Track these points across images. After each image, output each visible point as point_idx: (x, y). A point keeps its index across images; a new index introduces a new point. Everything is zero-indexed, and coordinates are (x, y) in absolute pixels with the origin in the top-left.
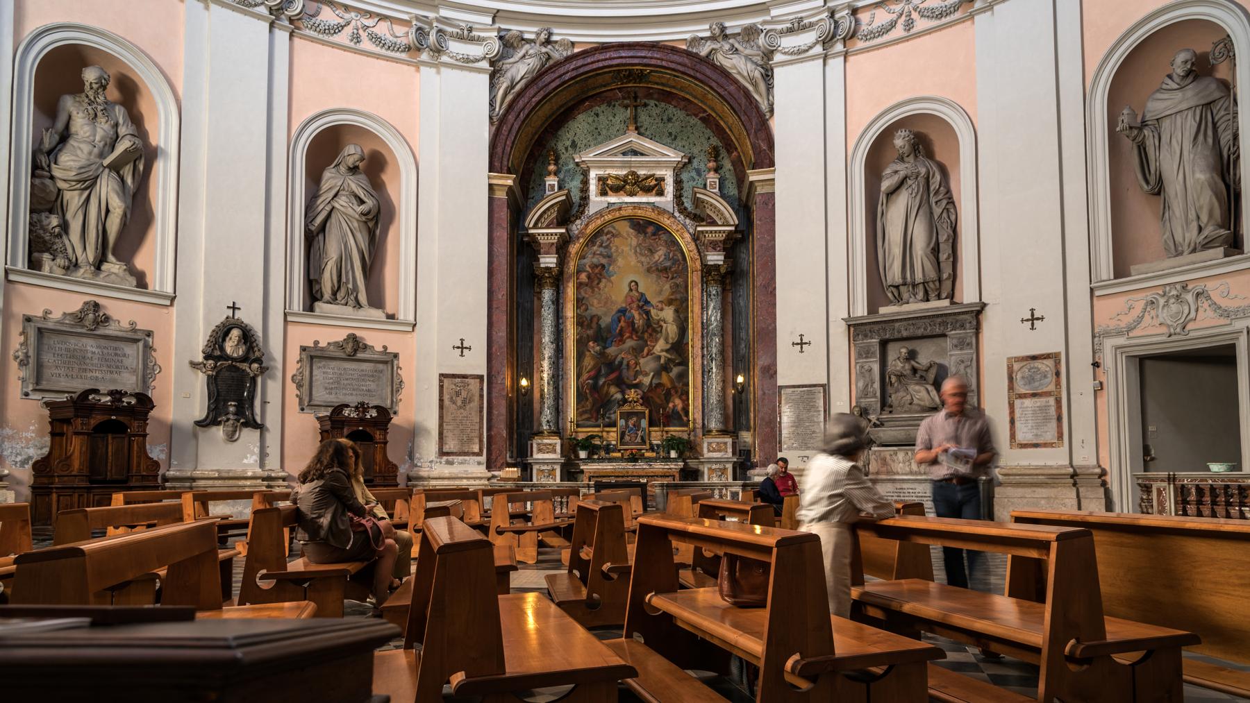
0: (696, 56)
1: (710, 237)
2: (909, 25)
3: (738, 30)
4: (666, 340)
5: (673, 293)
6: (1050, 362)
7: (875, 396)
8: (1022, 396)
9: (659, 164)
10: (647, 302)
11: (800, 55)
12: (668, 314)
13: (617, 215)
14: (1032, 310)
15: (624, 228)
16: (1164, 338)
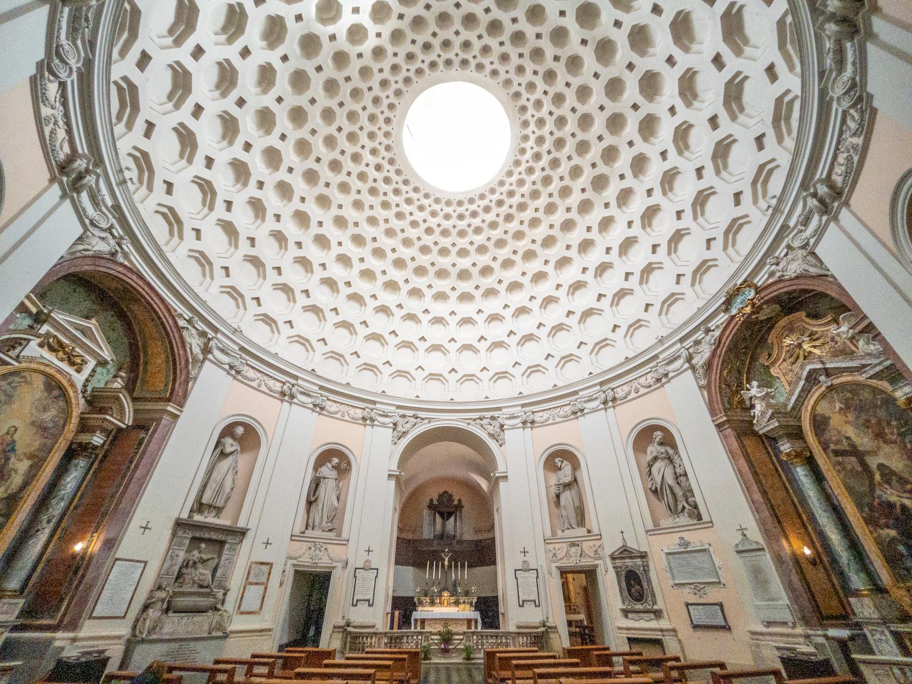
0: (176, 323)
1: (105, 425)
2: (260, 385)
3: (200, 329)
4: (6, 489)
5: (38, 450)
6: (268, 567)
8: (251, 584)
9: (92, 352)
10: (13, 450)
11: (218, 364)
12: (23, 466)
13: (42, 368)
15: (39, 381)
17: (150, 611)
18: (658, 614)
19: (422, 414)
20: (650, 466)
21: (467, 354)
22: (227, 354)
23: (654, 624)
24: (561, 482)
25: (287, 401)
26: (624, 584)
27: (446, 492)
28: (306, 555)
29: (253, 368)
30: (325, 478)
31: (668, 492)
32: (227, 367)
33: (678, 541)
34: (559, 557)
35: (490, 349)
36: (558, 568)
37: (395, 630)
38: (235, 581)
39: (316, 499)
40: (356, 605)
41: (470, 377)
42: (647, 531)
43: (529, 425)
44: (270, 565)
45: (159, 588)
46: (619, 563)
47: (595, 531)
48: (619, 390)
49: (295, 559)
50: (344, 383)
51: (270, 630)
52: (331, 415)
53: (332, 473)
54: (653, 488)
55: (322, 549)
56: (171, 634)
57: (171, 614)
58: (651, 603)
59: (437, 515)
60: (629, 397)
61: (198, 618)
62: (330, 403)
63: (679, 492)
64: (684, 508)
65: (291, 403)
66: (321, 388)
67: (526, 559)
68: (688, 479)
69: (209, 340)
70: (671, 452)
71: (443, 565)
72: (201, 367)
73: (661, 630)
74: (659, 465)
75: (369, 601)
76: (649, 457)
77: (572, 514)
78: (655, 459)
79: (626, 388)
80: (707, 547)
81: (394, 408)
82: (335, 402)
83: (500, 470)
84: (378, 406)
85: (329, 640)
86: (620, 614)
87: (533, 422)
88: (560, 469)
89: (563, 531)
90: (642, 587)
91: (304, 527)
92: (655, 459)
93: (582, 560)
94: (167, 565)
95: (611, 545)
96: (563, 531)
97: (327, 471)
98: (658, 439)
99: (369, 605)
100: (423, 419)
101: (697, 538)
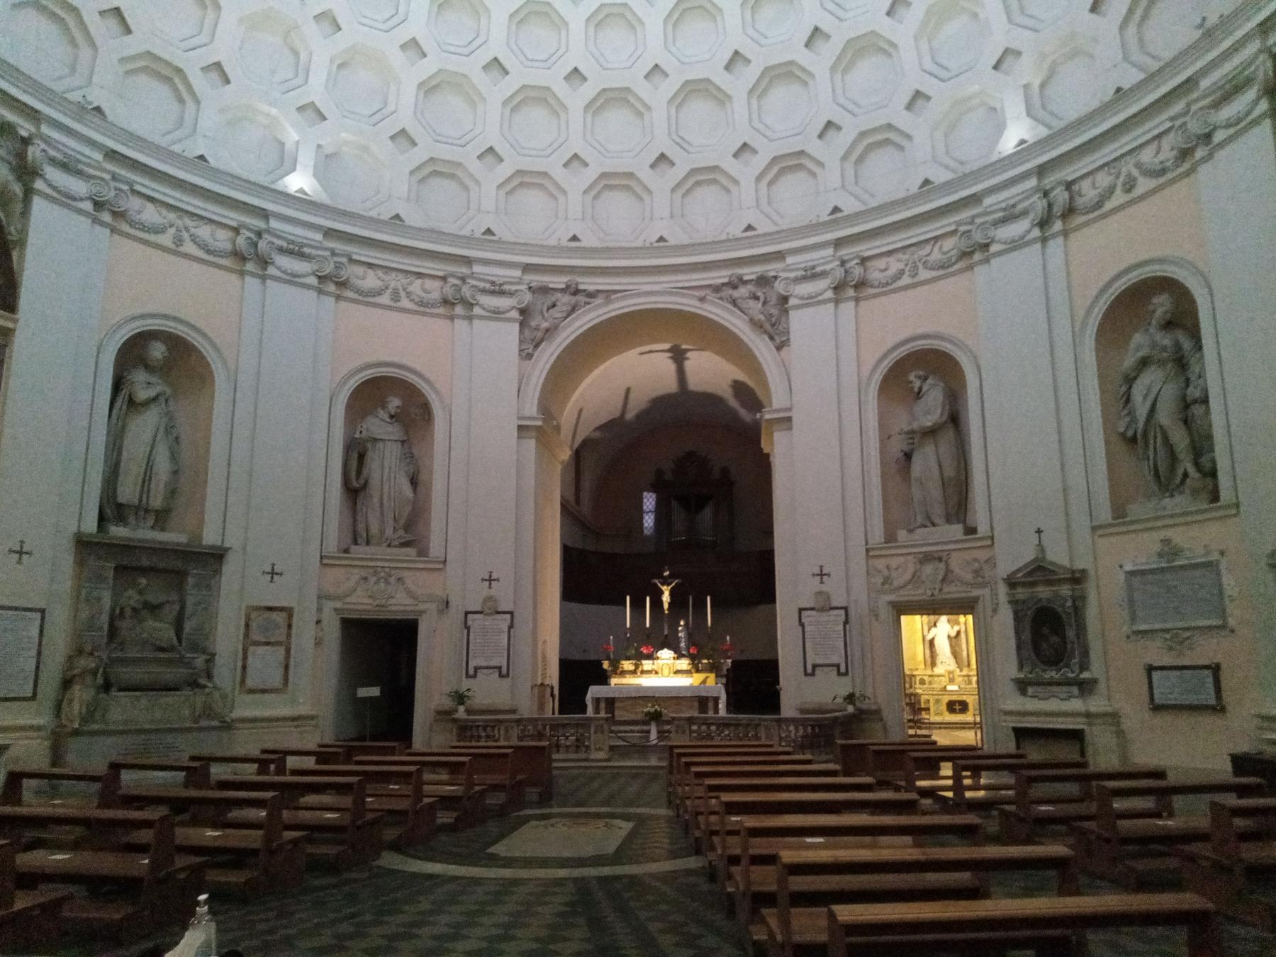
2: (179, 241)
6: (284, 614)
7: (101, 629)
11: (65, 199)
14: (273, 565)
16: (368, 607)
17: (76, 688)
18: (1086, 688)
19: (588, 283)
20: (1130, 380)
21: (699, 108)
22: (79, 173)
23: (1076, 705)
24: (915, 426)
25: (253, 274)
26: (1027, 636)
27: (691, 454)
28: (359, 592)
29: (151, 199)
30: (376, 440)
31: (1159, 440)
32: (88, 206)
33: (1157, 547)
34: (896, 584)
35: (759, 90)
36: (890, 603)
37: (557, 715)
38: (226, 638)
39: (365, 485)
40: (475, 676)
41: (706, 176)
42: (1094, 529)
43: (851, 292)
44: (289, 612)
45: (80, 652)
46: (1022, 593)
47: (983, 529)
48: (1085, 185)
49: (338, 598)
50: (386, 216)
51: (312, 718)
52: (367, 297)
53: (390, 429)
54: (1130, 433)
55: (392, 580)
56: (125, 722)
57: (114, 693)
58: (1076, 669)
59: (674, 503)
60: (1108, 206)
61: (170, 699)
62: (360, 270)
63: (1180, 438)
64: (1186, 475)
65: (263, 278)
66: (329, 233)
67: (824, 588)
68: (1208, 411)
69: (26, 142)
70: (1187, 345)
71: (657, 603)
72: (25, 213)
73: (1088, 715)
74: (1151, 379)
75: (500, 668)
76: (1129, 362)
77: (935, 492)
78: (1144, 363)
79: (1103, 180)
80: (1215, 556)
81: (518, 273)
82: (370, 265)
83: (775, 405)
84: (477, 269)
85: (426, 734)
86: (1011, 687)
87: (861, 284)
88: (919, 395)
89: (911, 531)
90: (1064, 638)
91: (349, 540)
92: (1144, 363)
93: (946, 589)
94: (84, 615)
95: (1012, 555)
96: (911, 531)
97: (378, 426)
98: (1159, 312)
99: (501, 676)
100: (592, 295)
101: (1198, 538)
